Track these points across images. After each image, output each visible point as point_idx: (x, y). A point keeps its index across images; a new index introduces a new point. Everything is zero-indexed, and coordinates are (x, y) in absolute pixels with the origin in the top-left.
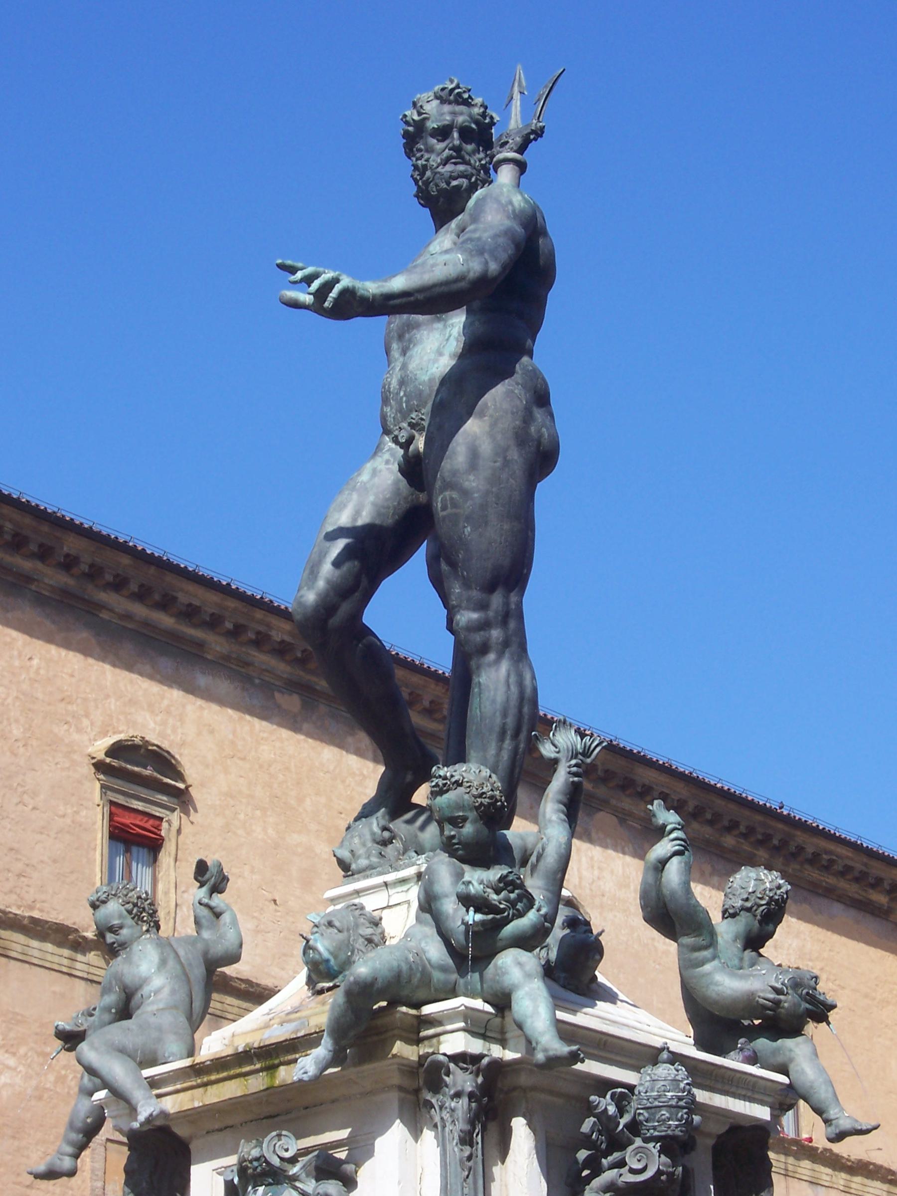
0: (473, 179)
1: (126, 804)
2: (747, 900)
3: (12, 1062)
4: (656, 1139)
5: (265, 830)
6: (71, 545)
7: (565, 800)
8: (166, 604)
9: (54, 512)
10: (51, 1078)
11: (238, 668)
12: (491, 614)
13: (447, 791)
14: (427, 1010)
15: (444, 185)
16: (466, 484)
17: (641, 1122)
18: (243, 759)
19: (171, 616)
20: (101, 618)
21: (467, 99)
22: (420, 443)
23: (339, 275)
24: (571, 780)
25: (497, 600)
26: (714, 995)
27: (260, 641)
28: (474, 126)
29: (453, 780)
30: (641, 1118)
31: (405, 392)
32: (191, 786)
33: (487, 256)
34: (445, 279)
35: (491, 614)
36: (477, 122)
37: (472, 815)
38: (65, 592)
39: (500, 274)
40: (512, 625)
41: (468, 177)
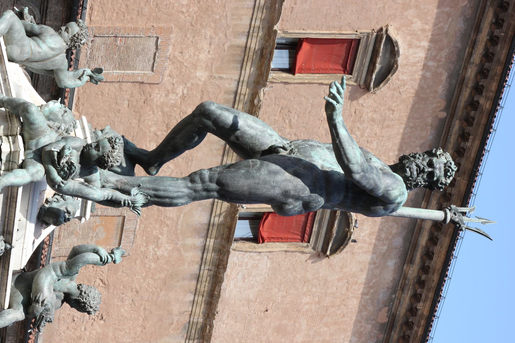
0: (410, 178)
1: (315, 221)
2: (85, 293)
5: (307, 303)
7: (113, 198)
9: (478, 171)
11: (400, 285)
12: (208, 183)
13: (110, 143)
14: (20, 138)
15: (407, 165)
16: (263, 170)
18: (347, 289)
19: (426, 244)
20: (422, 203)
21: (448, 175)
22: (283, 153)
23: (341, 104)
24: (122, 201)
25: (214, 186)
26: (41, 275)
27: (416, 297)
28: (435, 179)
29: (115, 145)
31: (307, 147)
32: (329, 258)
33: (362, 174)
34: (347, 153)
35: (208, 183)
36: (438, 180)
37: (100, 153)
39: (354, 179)
40: (204, 194)
41: (411, 176)
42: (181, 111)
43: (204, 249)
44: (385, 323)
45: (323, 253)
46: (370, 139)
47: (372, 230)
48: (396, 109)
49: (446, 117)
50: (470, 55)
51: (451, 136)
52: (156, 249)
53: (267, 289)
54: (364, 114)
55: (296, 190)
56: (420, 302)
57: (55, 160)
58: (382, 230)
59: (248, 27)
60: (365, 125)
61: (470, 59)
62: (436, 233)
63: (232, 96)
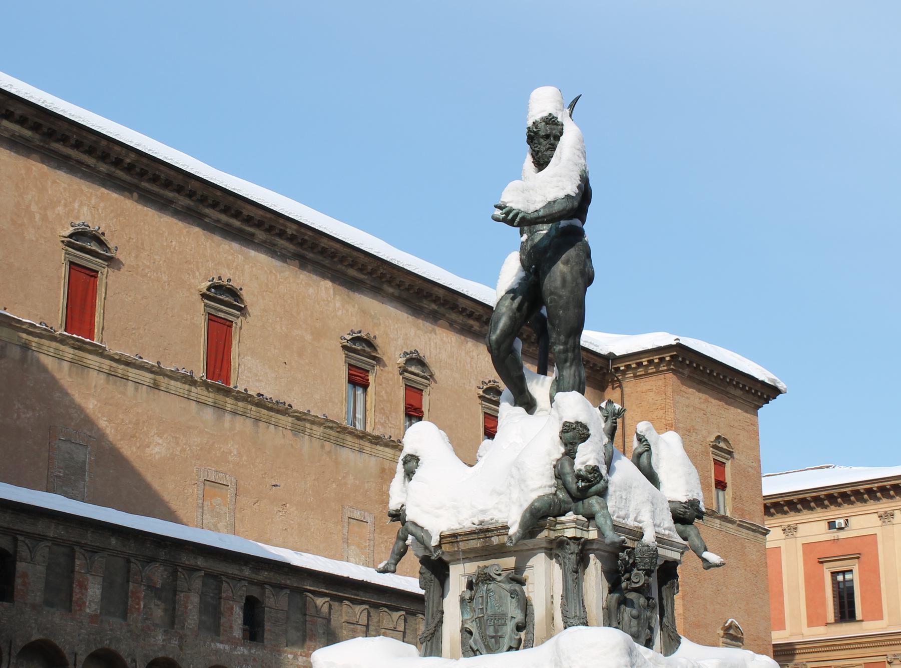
3: (160, 441)
4: (644, 570)
5: (281, 328)
6: (193, 185)
7: (611, 433)
8: (237, 215)
10: (179, 449)
11: (270, 247)
12: (569, 346)
17: (637, 563)
18: (271, 292)
19: (239, 221)
20: (206, 222)
29: (572, 427)
30: (637, 561)
31: (533, 251)
35: (569, 346)
38: (189, 209)
42: (121, 424)
43: (234, 413)
44: (300, 263)
45: (243, 311)
46: (152, 261)
47: (226, 266)
48: (128, 236)
49: (138, 193)
50: (88, 166)
51: (153, 190)
52: (232, 454)
53: (268, 361)
54: (132, 264)
55: (580, 263)
56: (286, 231)
57: (589, 485)
58: (226, 257)
59: (54, 358)
60: (141, 264)
61: (92, 167)
62: (233, 212)
63: (111, 378)
